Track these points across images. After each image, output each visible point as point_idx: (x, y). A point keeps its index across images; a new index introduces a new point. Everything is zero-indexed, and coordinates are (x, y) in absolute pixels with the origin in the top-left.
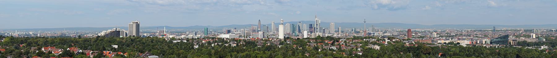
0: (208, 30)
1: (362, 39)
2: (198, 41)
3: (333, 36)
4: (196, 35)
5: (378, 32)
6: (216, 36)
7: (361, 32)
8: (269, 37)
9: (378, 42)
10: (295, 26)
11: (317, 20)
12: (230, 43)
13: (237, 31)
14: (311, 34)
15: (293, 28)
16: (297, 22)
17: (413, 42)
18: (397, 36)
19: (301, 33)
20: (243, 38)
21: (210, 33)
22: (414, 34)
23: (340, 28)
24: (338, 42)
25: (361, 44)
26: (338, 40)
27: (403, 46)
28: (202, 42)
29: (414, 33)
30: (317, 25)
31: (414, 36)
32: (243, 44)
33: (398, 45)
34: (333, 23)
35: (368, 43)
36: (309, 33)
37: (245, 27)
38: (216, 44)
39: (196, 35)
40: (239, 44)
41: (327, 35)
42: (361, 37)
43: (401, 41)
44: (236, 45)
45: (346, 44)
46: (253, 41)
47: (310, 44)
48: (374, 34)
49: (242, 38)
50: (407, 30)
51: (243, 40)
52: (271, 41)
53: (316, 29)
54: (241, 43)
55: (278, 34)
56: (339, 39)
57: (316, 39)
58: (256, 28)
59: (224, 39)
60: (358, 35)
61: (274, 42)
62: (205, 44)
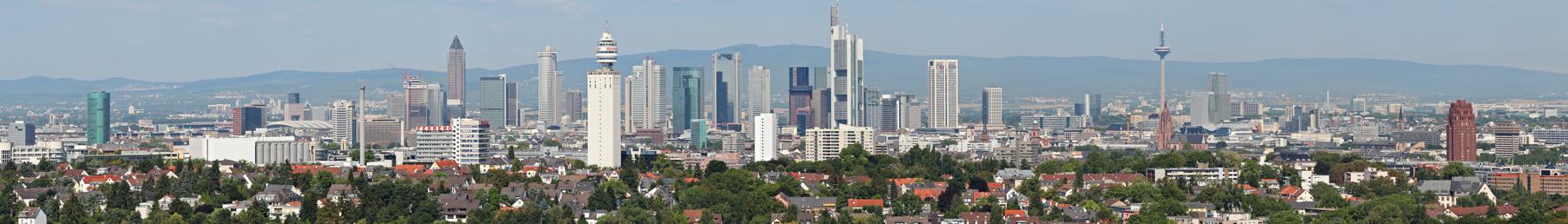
0: (113, 110)
1: (1144, 166)
2: (43, 183)
3: (951, 148)
4: (30, 140)
5: (1252, 121)
6: (165, 148)
7: (1136, 120)
8: (520, 155)
9: (1248, 191)
10: (693, 84)
11: (844, 42)
12: (260, 197)
13: (308, 116)
14: (802, 133)
15: (682, 94)
16: (709, 53)
17: (1485, 189)
18: (1379, 147)
19: (738, 128)
20: (348, 163)
21: (125, 129)
22: (1490, 138)
23: (995, 93)
24: (984, 188)
25: (1134, 201)
26: (979, 175)
27: (1420, 213)
28: (71, 191)
29: (1490, 132)
30: (841, 73)
31: (1492, 152)
32: (346, 206)
33: (1384, 207)
34: (946, 62)
35: (1183, 199)
36: (786, 130)
37: (359, 84)
38: (166, 201)
39: (30, 140)
40: (319, 203)
41: (905, 143)
42: (1138, 153)
43: (1402, 182)
44: (297, 211)
45: (1036, 206)
46: (415, 182)
47: (796, 201)
48: (1223, 132)
49: (338, 164)
50: (1442, 107)
51: (345, 177)
52: (537, 179)
53: (834, 99)
54: (335, 199)
55: (581, 138)
56: (992, 166)
57: (834, 167)
58: (431, 91)
59: (222, 168)
60: (1117, 138)
61: (552, 192)
62: (94, 200)
